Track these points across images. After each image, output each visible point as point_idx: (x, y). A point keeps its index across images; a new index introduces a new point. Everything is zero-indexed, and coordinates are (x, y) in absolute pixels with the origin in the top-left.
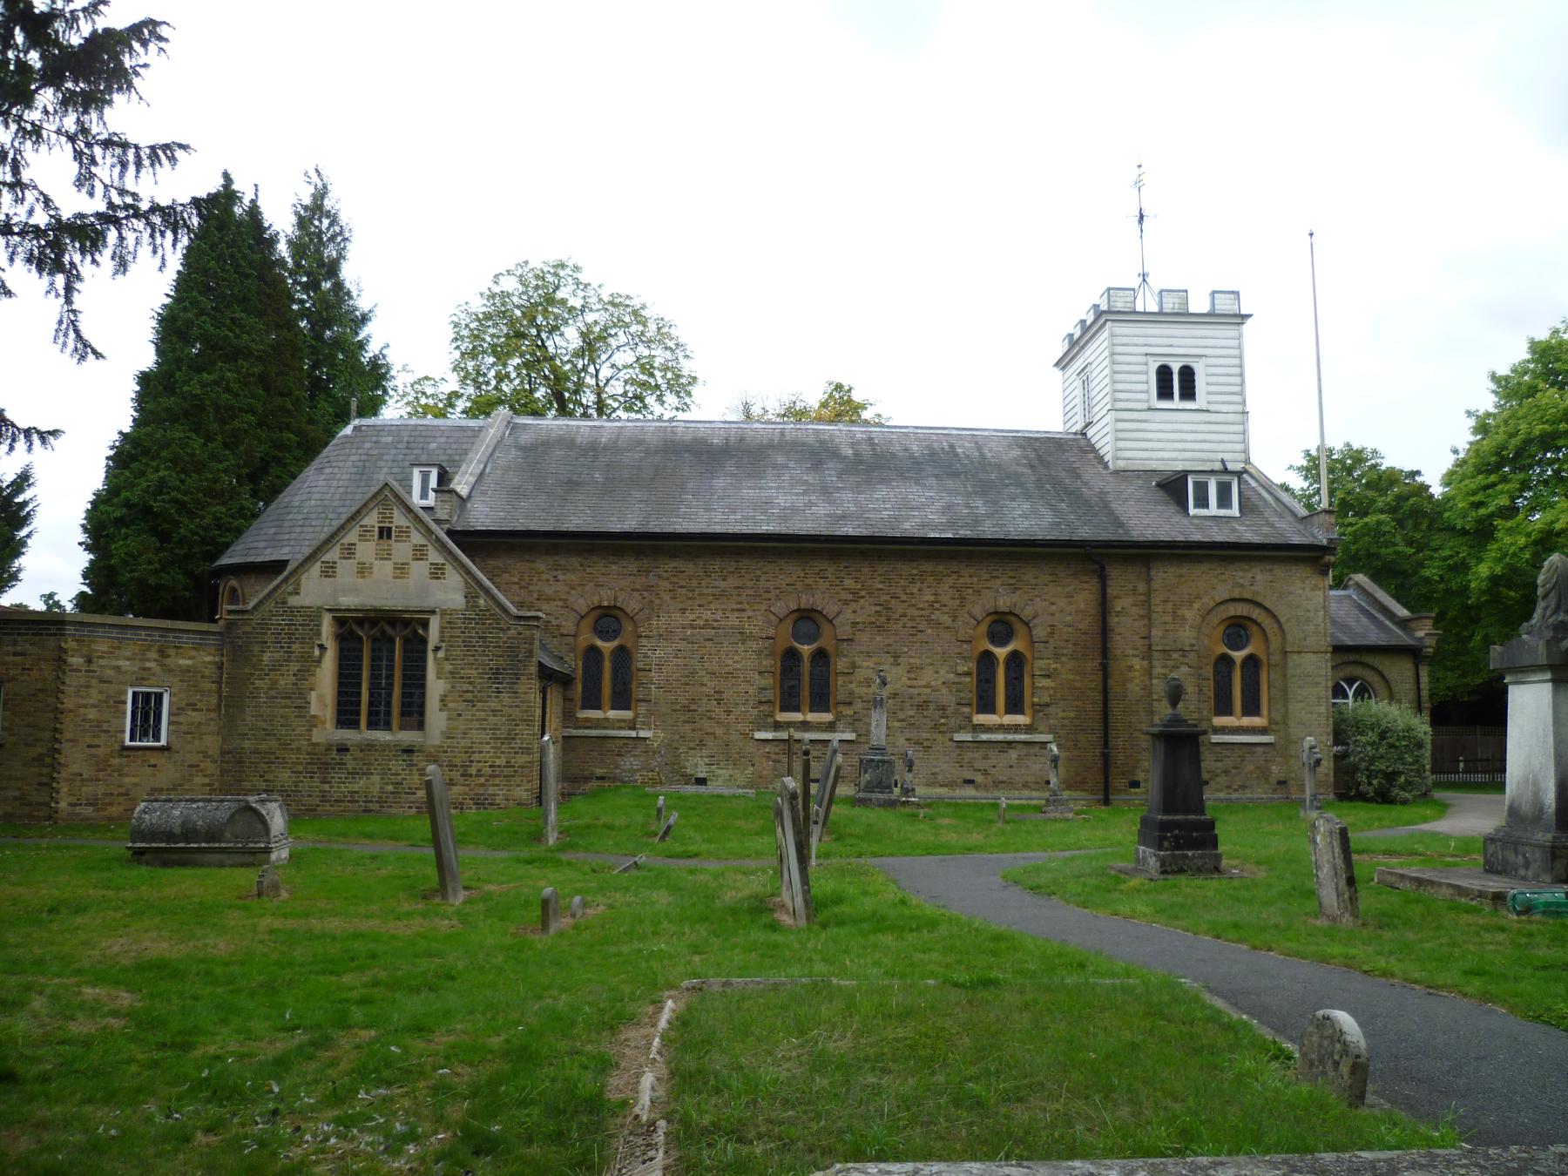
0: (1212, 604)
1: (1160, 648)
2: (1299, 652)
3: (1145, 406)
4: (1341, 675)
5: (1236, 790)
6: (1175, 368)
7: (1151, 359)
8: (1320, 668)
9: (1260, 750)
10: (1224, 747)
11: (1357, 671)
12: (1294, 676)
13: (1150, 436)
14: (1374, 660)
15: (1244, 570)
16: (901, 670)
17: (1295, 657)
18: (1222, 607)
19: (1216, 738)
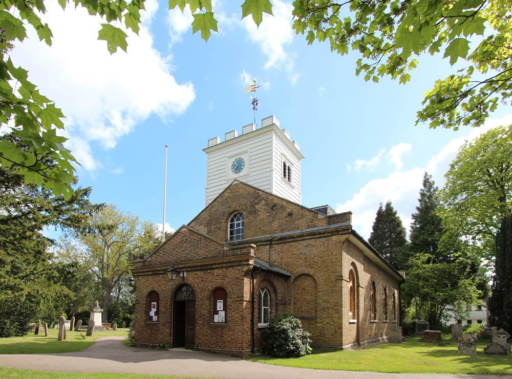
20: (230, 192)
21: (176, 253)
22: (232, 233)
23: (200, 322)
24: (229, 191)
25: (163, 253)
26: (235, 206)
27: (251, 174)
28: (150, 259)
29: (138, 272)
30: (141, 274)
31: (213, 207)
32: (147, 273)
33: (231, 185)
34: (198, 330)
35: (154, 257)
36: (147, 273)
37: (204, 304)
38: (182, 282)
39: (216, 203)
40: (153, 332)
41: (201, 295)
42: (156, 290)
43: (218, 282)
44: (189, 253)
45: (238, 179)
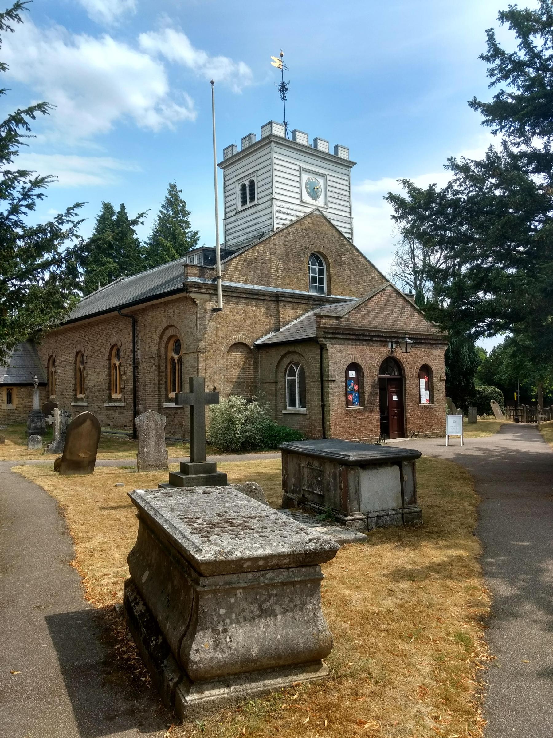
0: (162, 330)
1: (147, 357)
2: (188, 353)
3: (233, 213)
4: (289, 361)
5: (172, 434)
6: (247, 183)
7: (237, 184)
8: (195, 362)
9: (179, 411)
10: (170, 409)
11: (296, 358)
12: (186, 368)
13: (237, 229)
14: (299, 349)
15: (171, 309)
16: (95, 375)
17: (187, 356)
18: (167, 331)
19: (166, 405)
20: (310, 221)
21: (382, 316)
22: (321, 281)
23: (411, 404)
24: (309, 220)
25: (366, 312)
26: (318, 246)
27: (330, 210)
28: (347, 316)
29: (333, 333)
30: (339, 336)
31: (289, 233)
32: (348, 337)
33: (312, 213)
34: (410, 413)
35: (353, 315)
36: (348, 337)
37: (414, 383)
38: (389, 354)
39: (293, 229)
40: (358, 422)
41: (411, 372)
42: (359, 361)
43: (426, 360)
44: (396, 319)
45: (320, 209)
